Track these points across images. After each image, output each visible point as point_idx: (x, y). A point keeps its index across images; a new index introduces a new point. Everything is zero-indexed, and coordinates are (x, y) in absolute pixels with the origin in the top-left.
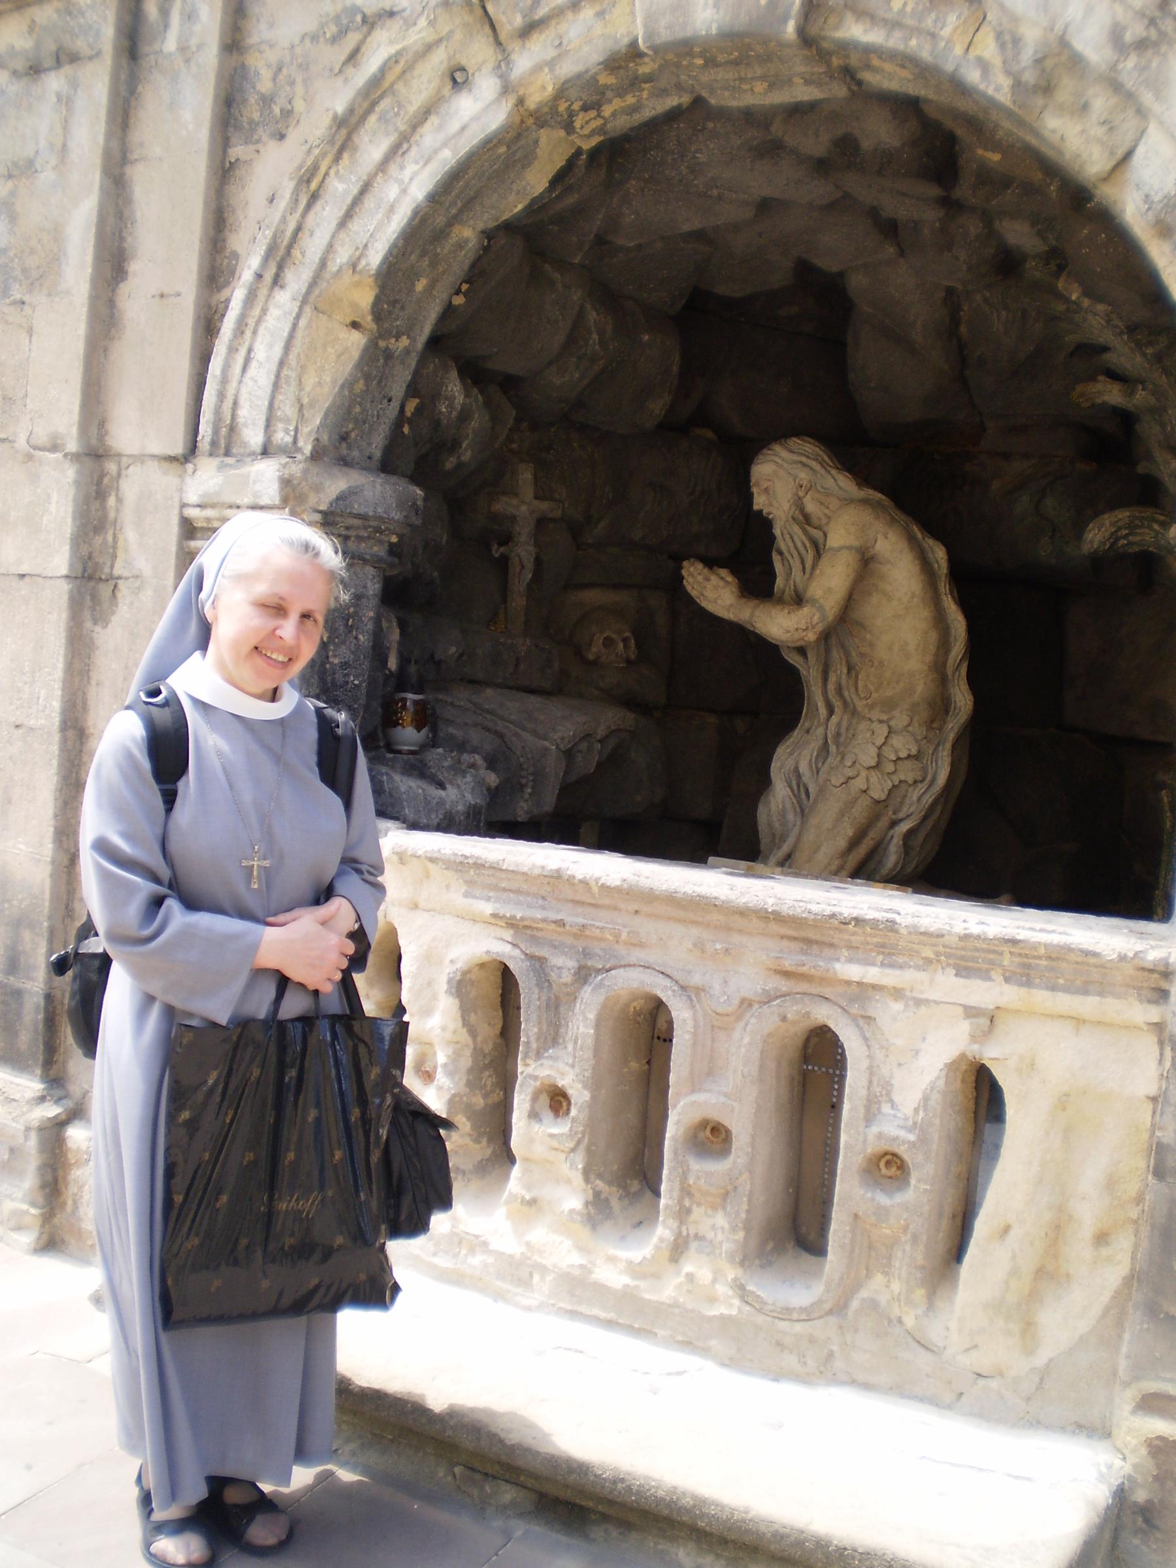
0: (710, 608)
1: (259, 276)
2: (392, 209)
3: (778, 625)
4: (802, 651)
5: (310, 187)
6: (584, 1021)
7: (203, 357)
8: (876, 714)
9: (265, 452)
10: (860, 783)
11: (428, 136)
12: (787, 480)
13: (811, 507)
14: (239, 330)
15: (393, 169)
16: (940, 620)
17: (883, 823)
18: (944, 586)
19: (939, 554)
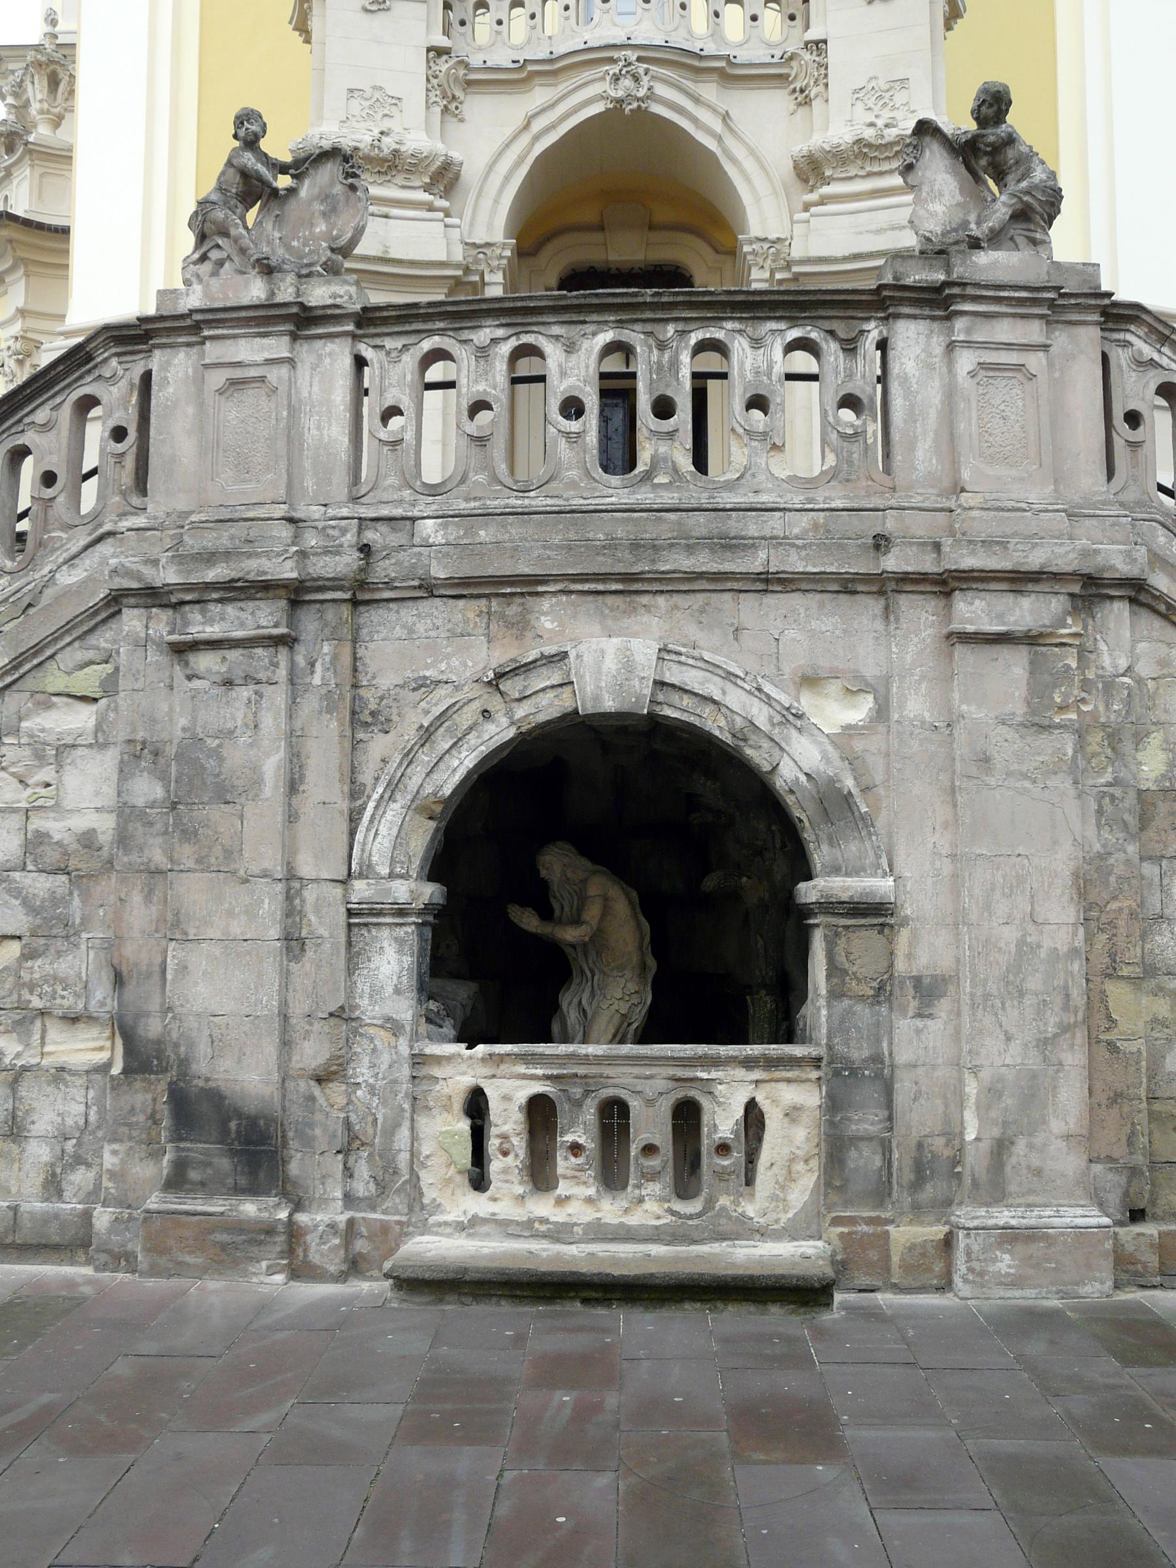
0: (526, 927)
1: (382, 797)
2: (455, 770)
3: (570, 934)
4: (573, 946)
5: (409, 757)
6: (590, 1113)
7: (352, 833)
8: (615, 973)
9: (392, 876)
10: (615, 1007)
11: (472, 738)
12: (558, 864)
13: (569, 875)
14: (371, 821)
15: (454, 752)
16: (639, 926)
17: (626, 1024)
18: (638, 910)
19: (634, 894)
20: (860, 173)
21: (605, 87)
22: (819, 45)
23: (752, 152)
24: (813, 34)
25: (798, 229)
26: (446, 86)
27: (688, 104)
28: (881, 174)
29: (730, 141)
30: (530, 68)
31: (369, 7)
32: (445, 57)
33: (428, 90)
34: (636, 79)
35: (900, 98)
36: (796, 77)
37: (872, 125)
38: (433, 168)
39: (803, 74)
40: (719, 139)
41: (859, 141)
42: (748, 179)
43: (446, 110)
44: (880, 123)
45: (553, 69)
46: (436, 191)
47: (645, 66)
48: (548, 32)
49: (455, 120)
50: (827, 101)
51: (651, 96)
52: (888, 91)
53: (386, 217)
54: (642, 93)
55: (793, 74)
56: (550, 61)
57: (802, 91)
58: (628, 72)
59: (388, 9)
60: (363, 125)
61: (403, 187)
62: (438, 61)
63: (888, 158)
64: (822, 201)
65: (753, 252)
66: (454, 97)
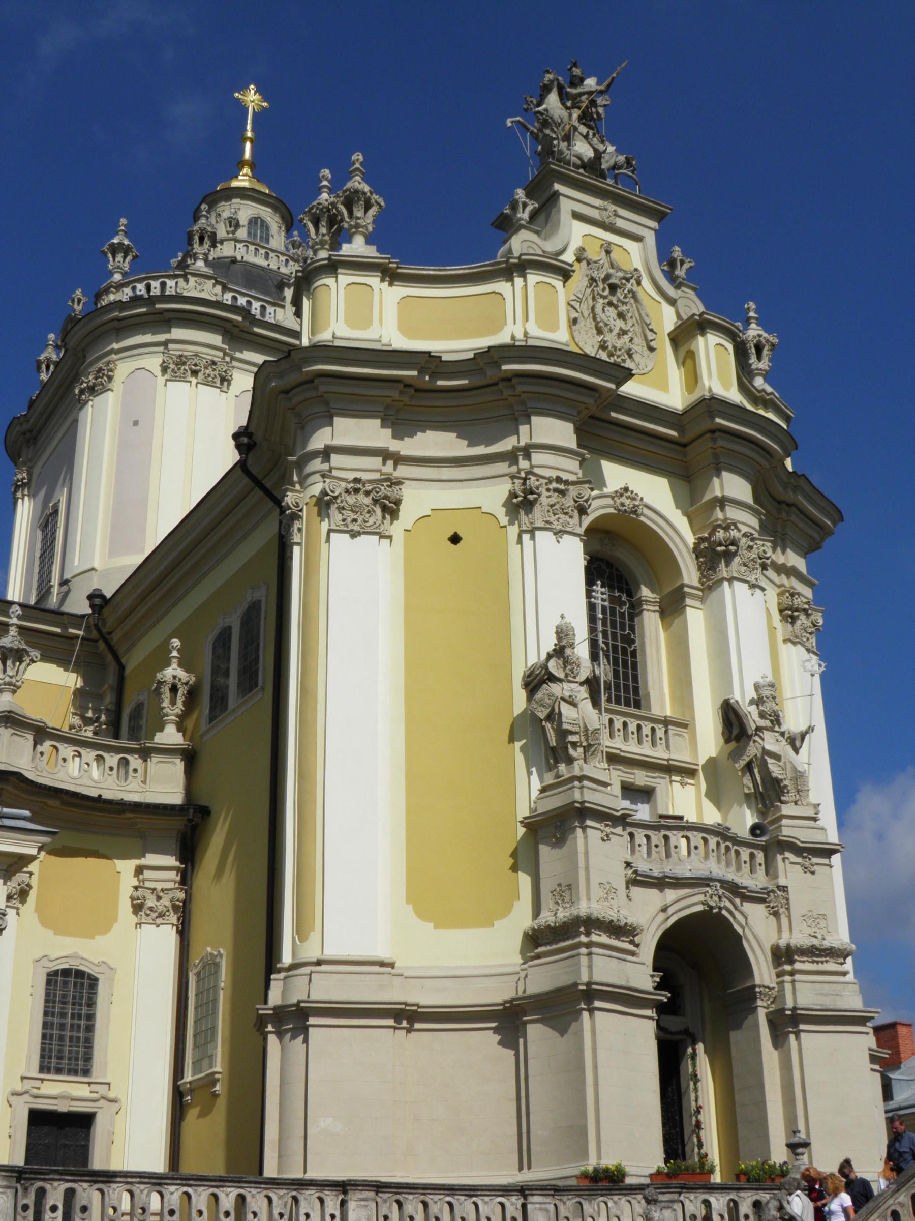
22: (784, 889)
23: (755, 937)
24: (782, 881)
25: (788, 987)
27: (733, 909)
28: (818, 962)
29: (747, 930)
34: (720, 898)
35: (823, 924)
40: (744, 929)
41: (813, 946)
44: (820, 937)
45: (678, 883)
53: (625, 960)
64: (792, 973)
65: (760, 992)
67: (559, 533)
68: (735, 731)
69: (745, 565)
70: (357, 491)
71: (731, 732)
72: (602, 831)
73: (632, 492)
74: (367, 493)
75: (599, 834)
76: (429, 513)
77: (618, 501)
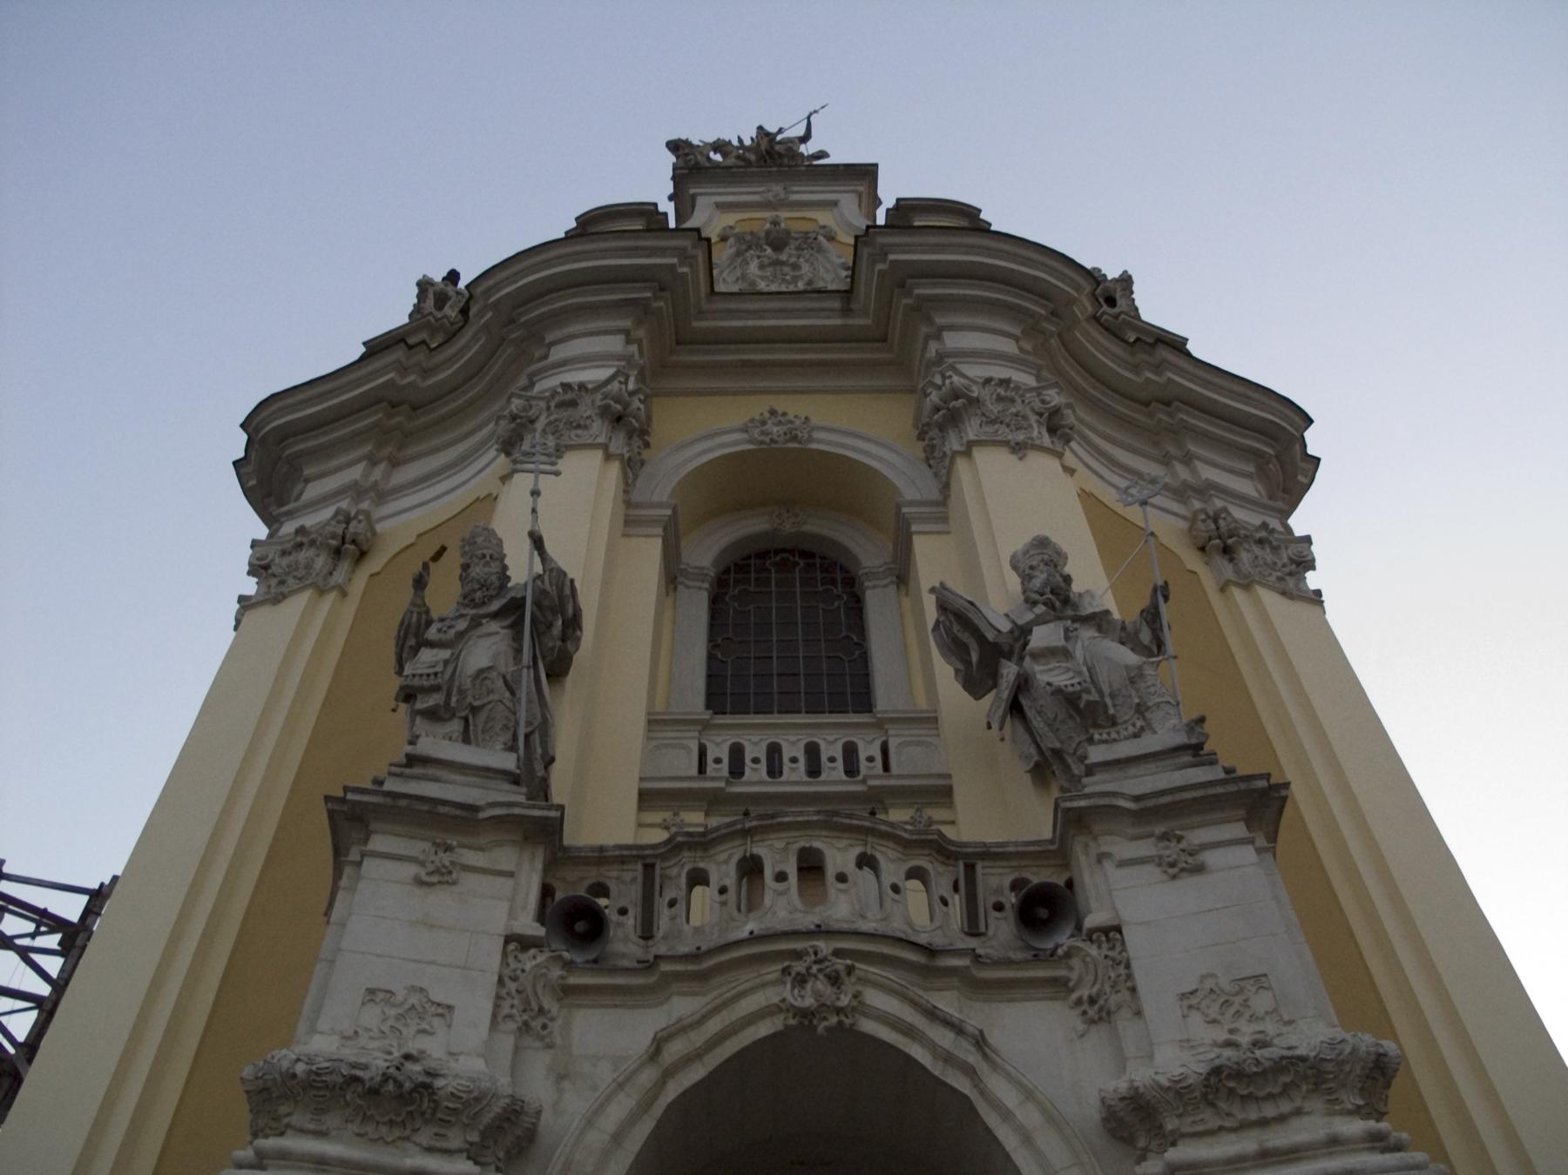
20: (1228, 1124)
21: (787, 992)
22: (1112, 932)
23: (1029, 1094)
26: (530, 991)
28: (1263, 1123)
30: (666, 967)
31: (425, 878)
32: (533, 951)
33: (498, 997)
34: (835, 980)
35: (1261, 1002)
36: (1080, 981)
37: (1229, 1044)
38: (487, 1118)
39: (1091, 978)
41: (1216, 1071)
42: (1027, 1139)
43: (525, 1028)
44: (1244, 1040)
46: (489, 1160)
47: (849, 962)
48: (695, 920)
49: (538, 1044)
50: (1138, 1013)
51: (860, 1007)
52: (1237, 994)
54: (845, 1001)
55: (1074, 976)
56: (697, 956)
57: (1092, 1001)
58: (820, 970)
59: (454, 883)
60: (376, 1044)
61: (430, 1150)
62: (522, 957)
63: (1271, 1097)
66: (541, 1011)
67: (559, 451)
68: (975, 657)
69: (993, 422)
70: (300, 546)
71: (968, 663)
72: (422, 864)
73: (784, 414)
74: (313, 543)
75: (410, 870)
76: (413, 540)
77: (756, 433)
